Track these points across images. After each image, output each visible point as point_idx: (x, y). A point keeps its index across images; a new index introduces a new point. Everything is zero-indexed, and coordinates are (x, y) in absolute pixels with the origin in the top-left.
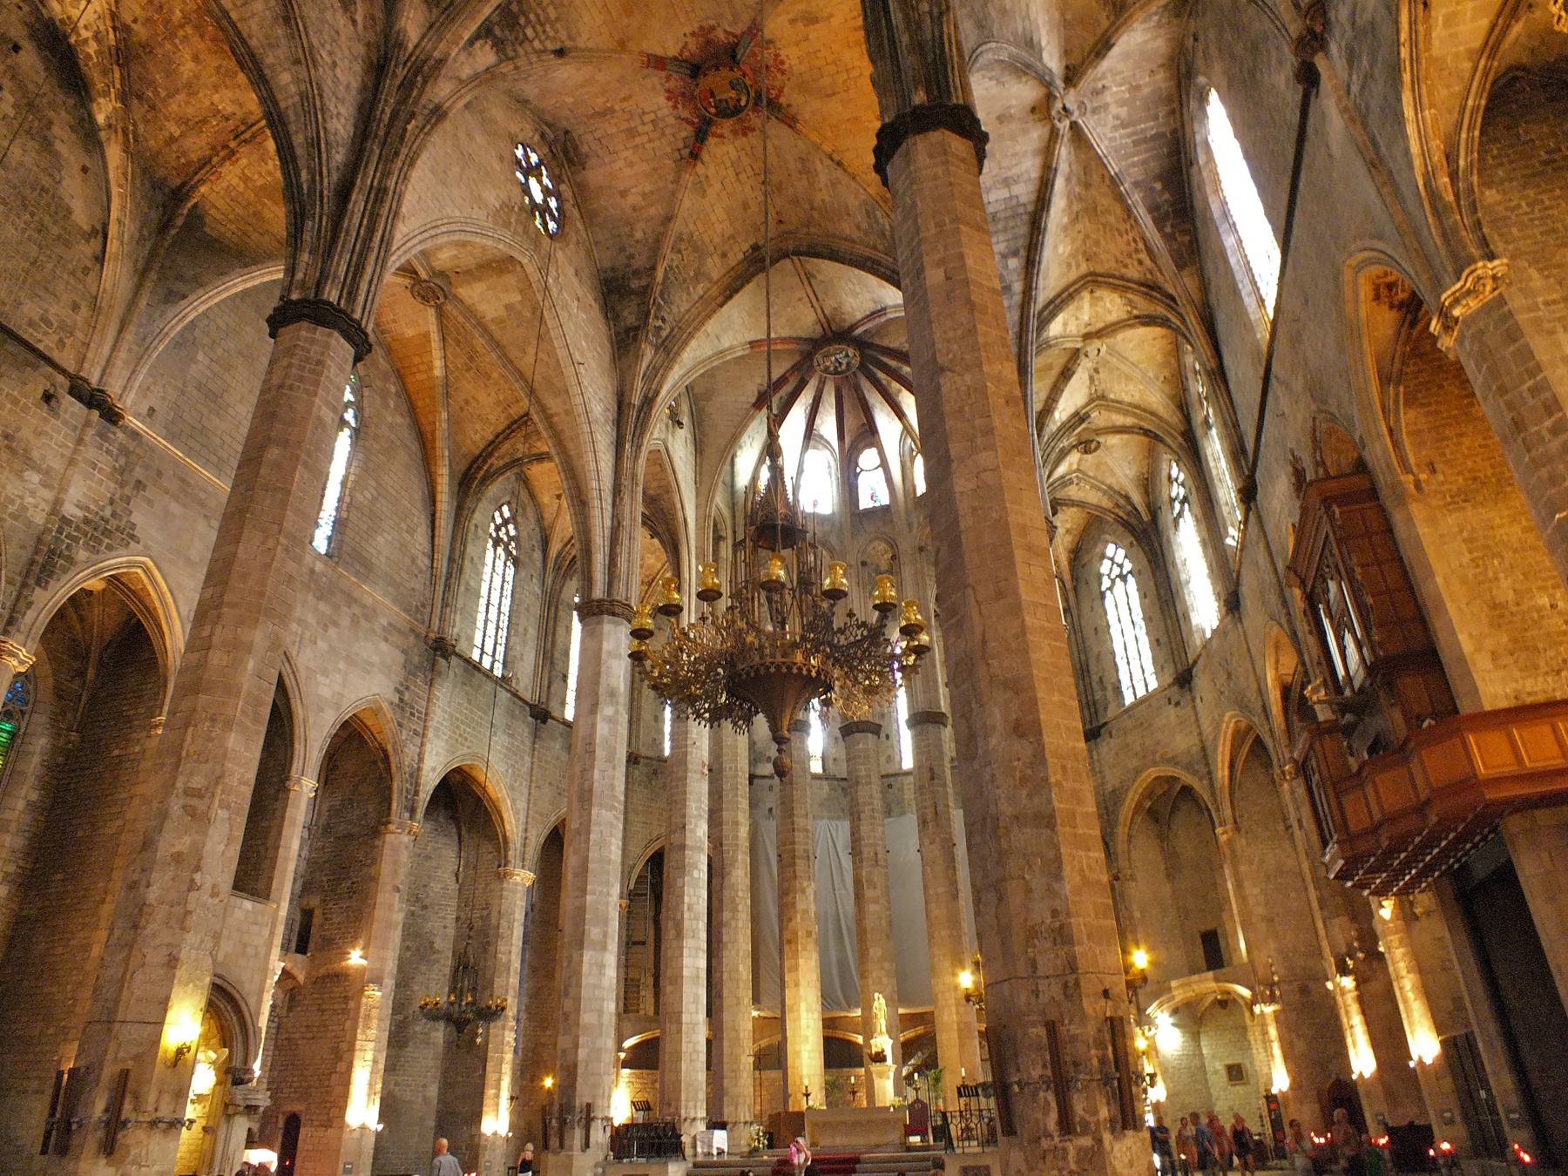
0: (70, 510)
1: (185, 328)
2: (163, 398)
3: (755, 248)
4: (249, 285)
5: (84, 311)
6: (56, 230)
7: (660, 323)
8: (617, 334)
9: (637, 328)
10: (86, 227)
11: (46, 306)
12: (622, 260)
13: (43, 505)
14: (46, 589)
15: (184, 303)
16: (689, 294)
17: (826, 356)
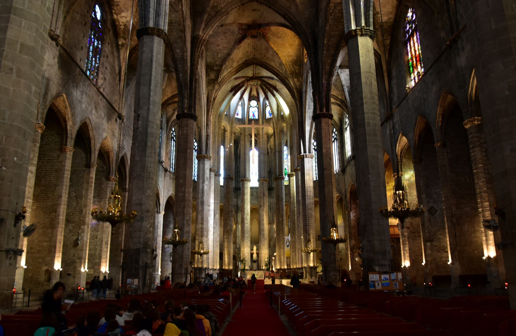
3: (246, 61)
8: (208, 80)
9: (214, 80)
12: (213, 61)
17: (251, 82)
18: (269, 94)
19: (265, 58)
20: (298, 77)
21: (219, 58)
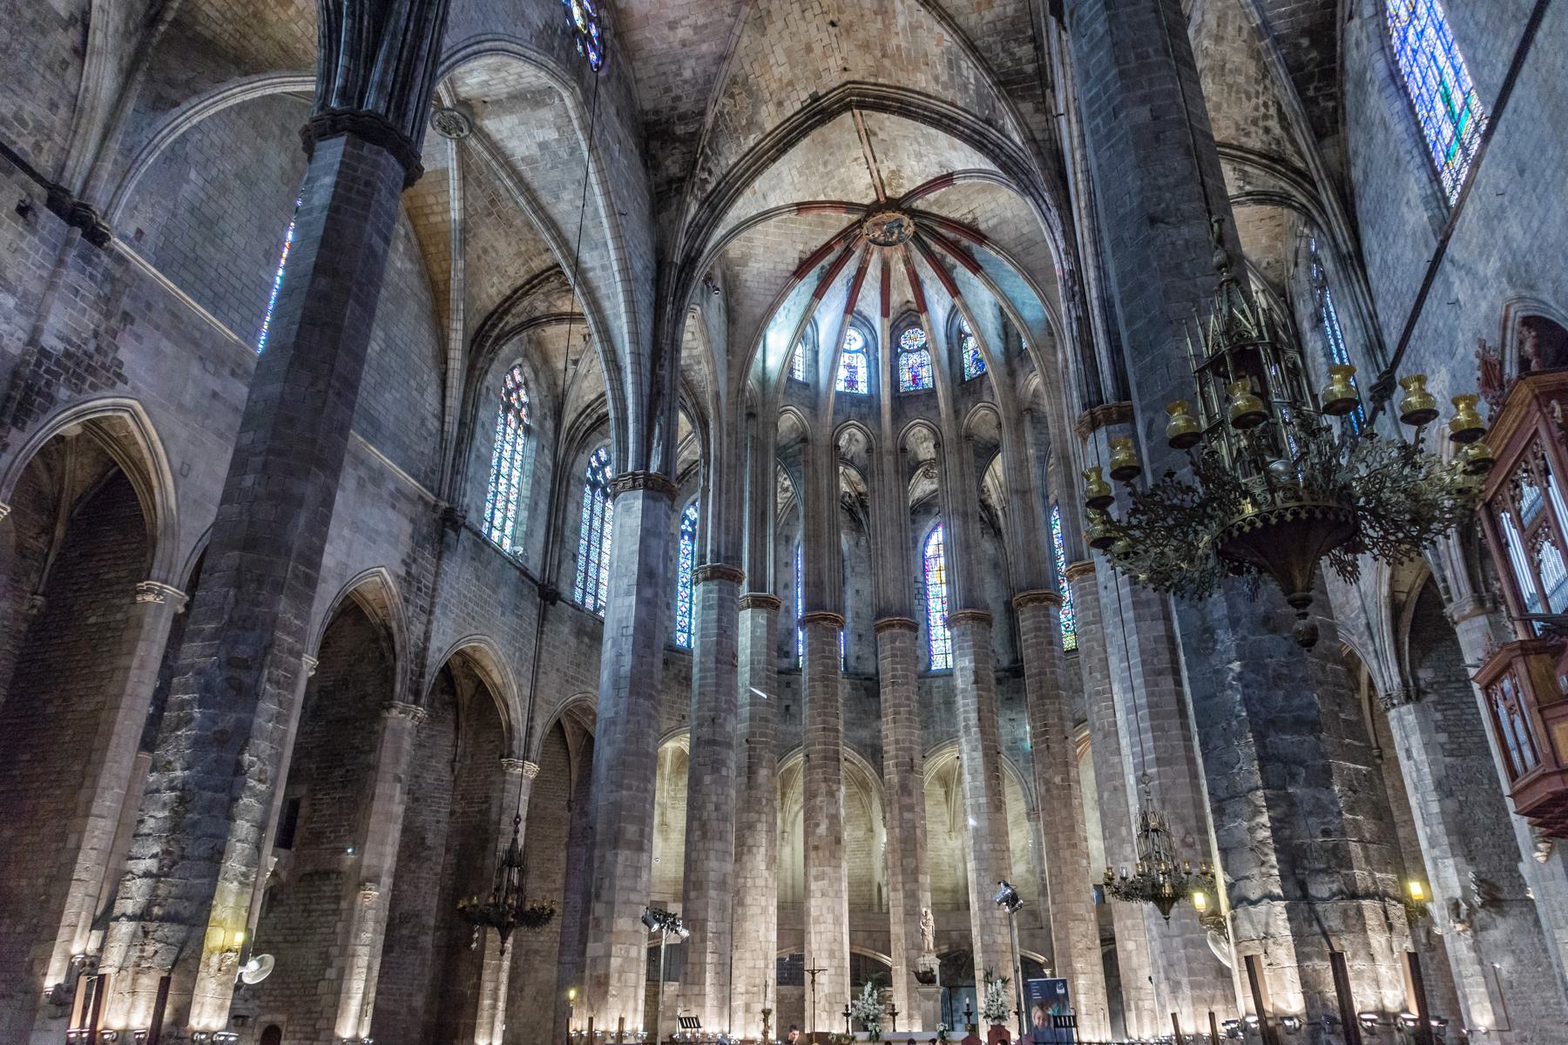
0: (50, 341)
1: (176, 141)
2: (152, 220)
3: (815, 98)
4: (249, 97)
5: (63, 112)
6: (28, 14)
7: (705, 175)
9: (682, 180)
10: (64, 14)
11: (19, 101)
12: (666, 101)
13: (20, 334)
14: (22, 429)
15: (176, 111)
16: (739, 145)
18: (962, 273)
19: (887, 62)
20: (1039, 92)
21: (685, 82)
